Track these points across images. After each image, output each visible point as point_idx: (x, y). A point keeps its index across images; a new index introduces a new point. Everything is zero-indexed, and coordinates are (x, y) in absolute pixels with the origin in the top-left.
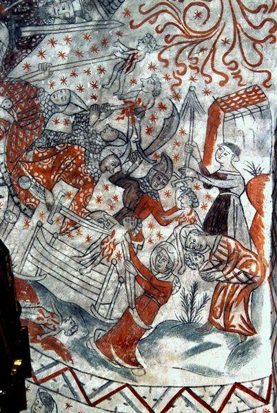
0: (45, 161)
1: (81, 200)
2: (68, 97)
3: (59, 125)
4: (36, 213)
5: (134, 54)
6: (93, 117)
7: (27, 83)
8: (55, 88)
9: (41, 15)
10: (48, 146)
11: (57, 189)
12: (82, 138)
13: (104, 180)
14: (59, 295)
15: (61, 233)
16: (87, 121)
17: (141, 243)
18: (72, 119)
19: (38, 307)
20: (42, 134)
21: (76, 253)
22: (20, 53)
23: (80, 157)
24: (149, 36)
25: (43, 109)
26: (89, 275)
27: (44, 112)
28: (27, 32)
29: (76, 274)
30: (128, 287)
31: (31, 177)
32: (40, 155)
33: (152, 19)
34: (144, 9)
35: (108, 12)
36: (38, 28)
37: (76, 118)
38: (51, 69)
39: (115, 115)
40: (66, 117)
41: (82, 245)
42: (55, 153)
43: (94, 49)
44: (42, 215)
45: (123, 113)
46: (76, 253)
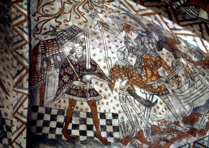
0: (148, 72)
1: (167, 67)
2: (121, 53)
3: (133, 61)
4: (168, 89)
5: (100, 22)
6: (131, 45)
7: (112, 69)
8: (116, 57)
9: (81, 60)
10: (141, 69)
11: (161, 74)
12: (140, 53)
13: (160, 53)
14: (202, 104)
15: (179, 85)
16: (133, 48)
17: (188, 57)
18: (131, 54)
19: (204, 115)
20: (136, 68)
21: (187, 84)
22: (98, 70)
23: (148, 57)
24: (90, 16)
25: (125, 65)
26: (198, 86)
27: (126, 65)
28: (88, 66)
29: (196, 91)
30: (207, 74)
31: (153, 82)
32: (145, 74)
33: (82, 14)
34: (78, 17)
35: (80, 31)
36: (87, 62)
37: (130, 52)
38: (107, 57)
39: (129, 36)
40: (130, 56)
41: (185, 80)
42: (145, 67)
43: (98, 38)
44: (169, 87)
45: (129, 32)
46: (187, 84)
